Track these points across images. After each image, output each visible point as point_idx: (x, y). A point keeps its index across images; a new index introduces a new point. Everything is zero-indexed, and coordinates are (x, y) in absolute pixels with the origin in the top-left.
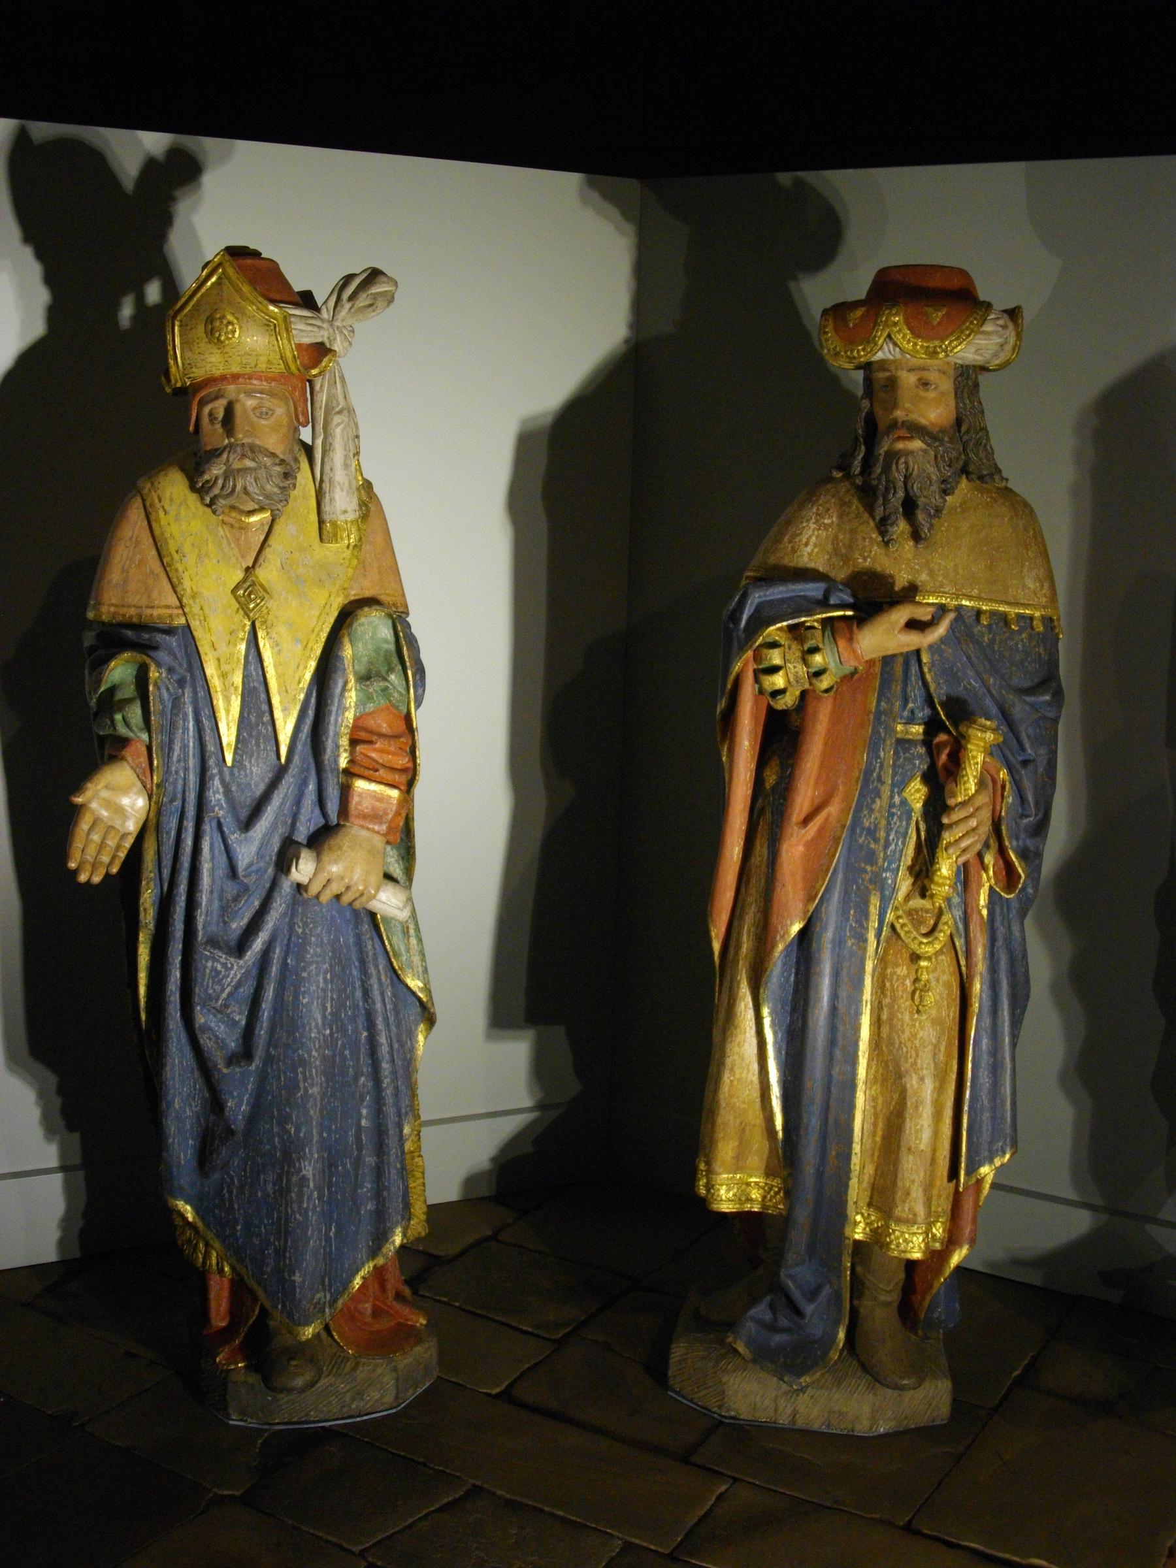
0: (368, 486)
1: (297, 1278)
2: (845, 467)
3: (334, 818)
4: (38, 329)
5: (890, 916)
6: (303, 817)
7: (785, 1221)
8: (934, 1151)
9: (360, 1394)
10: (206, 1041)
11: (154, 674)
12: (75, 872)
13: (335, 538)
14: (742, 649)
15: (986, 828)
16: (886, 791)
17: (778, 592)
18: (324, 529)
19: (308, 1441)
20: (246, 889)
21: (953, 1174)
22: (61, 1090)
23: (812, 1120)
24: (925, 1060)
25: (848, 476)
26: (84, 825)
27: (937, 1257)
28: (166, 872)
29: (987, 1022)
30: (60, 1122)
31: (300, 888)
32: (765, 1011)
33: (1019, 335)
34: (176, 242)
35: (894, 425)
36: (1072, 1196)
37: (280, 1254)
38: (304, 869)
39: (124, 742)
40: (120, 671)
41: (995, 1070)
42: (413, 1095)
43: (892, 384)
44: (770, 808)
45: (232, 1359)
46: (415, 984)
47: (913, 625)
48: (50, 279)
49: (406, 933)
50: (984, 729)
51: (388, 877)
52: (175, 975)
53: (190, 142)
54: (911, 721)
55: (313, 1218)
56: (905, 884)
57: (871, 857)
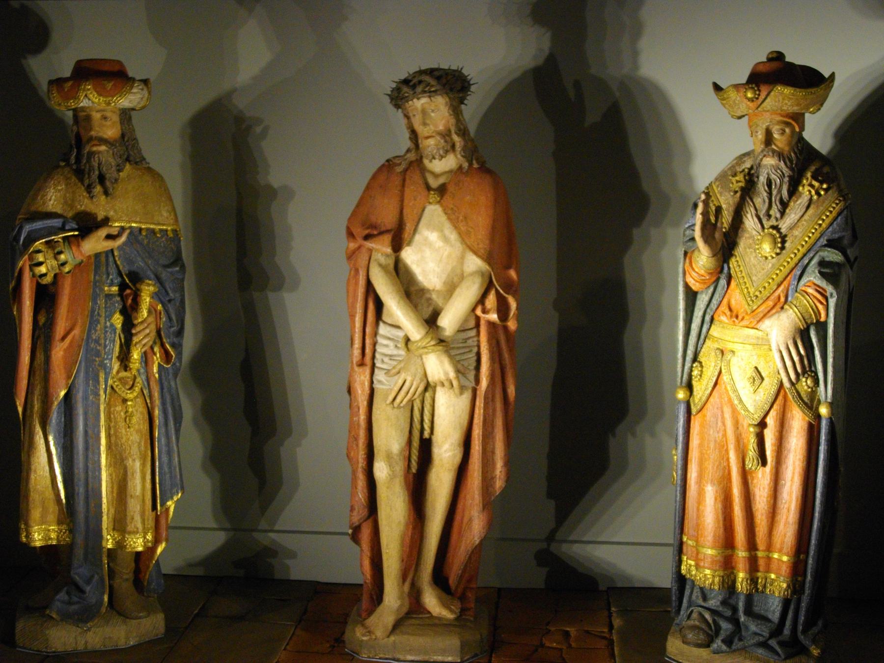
2: (67, 160)
5: (110, 382)
7: (71, 547)
8: (143, 496)
14: (22, 254)
15: (154, 334)
16: (102, 320)
17: (38, 225)
21: (154, 507)
23: (81, 490)
24: (135, 450)
25: (68, 164)
27: (151, 550)
29: (163, 430)
33: (150, 93)
35: (91, 139)
36: (215, 526)
41: (169, 453)
43: (88, 118)
44: (43, 335)
47: (109, 237)
50: (149, 285)
54: (111, 285)
56: (116, 366)
57: (98, 354)
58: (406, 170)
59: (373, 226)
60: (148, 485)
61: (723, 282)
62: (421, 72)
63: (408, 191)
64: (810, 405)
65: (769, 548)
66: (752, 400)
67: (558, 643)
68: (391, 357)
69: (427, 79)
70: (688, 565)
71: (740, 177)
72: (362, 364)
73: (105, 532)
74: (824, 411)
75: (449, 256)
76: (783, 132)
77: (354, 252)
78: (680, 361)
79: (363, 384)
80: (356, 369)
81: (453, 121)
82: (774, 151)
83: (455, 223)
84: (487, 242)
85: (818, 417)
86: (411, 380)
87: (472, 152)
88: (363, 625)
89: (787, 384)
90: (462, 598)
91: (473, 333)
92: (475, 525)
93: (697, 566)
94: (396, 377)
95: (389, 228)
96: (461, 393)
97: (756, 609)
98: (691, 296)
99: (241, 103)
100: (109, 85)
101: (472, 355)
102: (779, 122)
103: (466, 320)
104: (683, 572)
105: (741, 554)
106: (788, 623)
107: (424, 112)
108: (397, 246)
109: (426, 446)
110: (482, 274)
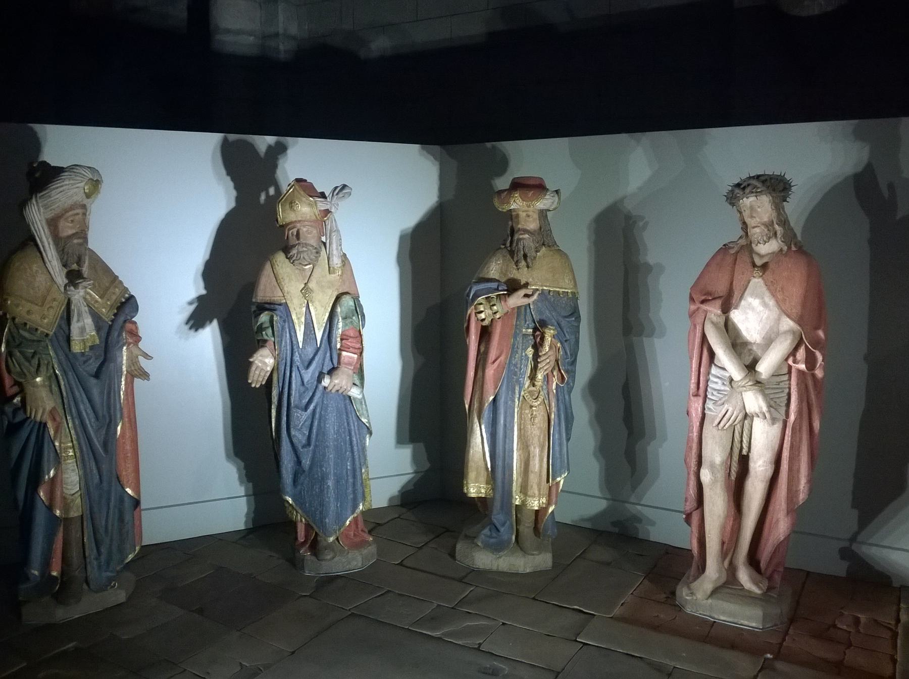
0: (345, 255)
1: (327, 520)
2: (504, 244)
3: (336, 365)
4: (233, 204)
5: (522, 393)
6: (326, 364)
7: (493, 499)
8: (540, 472)
9: (349, 563)
10: (294, 440)
11: (275, 318)
12: (251, 384)
13: (334, 273)
14: (471, 305)
15: (553, 363)
16: (520, 351)
17: (482, 286)
18: (331, 270)
19: (331, 579)
20: (307, 389)
21: (548, 481)
22: (246, 468)
23: (499, 463)
24: (536, 440)
25: (506, 247)
26: (253, 368)
28: (281, 385)
29: (557, 428)
30: (245, 479)
31: (325, 388)
32: (483, 427)
33: (559, 199)
34: (279, 174)
35: (519, 230)
36: (599, 495)
37: (321, 513)
38: (326, 382)
39: (265, 341)
40: (264, 318)
41: (561, 445)
42: (365, 459)
43: (517, 216)
45: (305, 552)
46: (365, 421)
47: (526, 296)
48: (236, 188)
49: (361, 403)
50: (550, 329)
51: (354, 384)
52: (284, 419)
53: (282, 139)
54: (528, 328)
55: (332, 500)
58: (737, 252)
59: (709, 293)
60: (545, 466)
67: (847, 626)
68: (718, 391)
69: (754, 182)
72: (697, 395)
73: (514, 494)
75: (768, 318)
77: (694, 312)
79: (697, 409)
80: (692, 398)
81: (774, 214)
83: (773, 295)
84: (799, 308)
86: (732, 410)
90: (770, 578)
91: (786, 378)
92: (781, 526)
96: (773, 424)
99: (629, 206)
100: (530, 194)
101: (785, 394)
103: (779, 367)
107: (752, 208)
108: (726, 309)
109: (744, 461)
110: (794, 333)
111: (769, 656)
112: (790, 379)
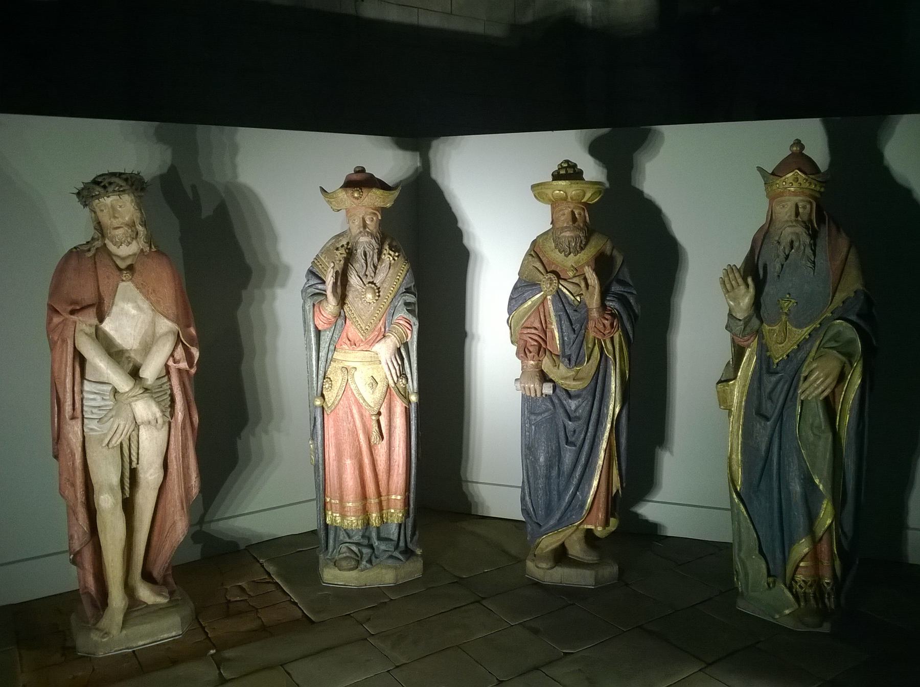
58: (95, 255)
59: (76, 303)
61: (340, 322)
62: (114, 174)
63: (100, 272)
64: (405, 397)
65: (388, 493)
66: (372, 398)
69: (117, 180)
70: (333, 517)
71: (342, 251)
72: (73, 418)
74: (414, 398)
76: (372, 221)
78: (315, 379)
79: (75, 433)
82: (368, 233)
84: (174, 308)
85: (410, 402)
86: (122, 425)
87: (150, 241)
88: (97, 629)
89: (392, 384)
91: (165, 379)
93: (343, 516)
94: (109, 424)
95: (90, 302)
97: (382, 535)
98: (318, 333)
102: (803, 201)
104: (328, 521)
105: (373, 501)
106: (402, 538)
109: (134, 473)
111: (212, 652)
112: (169, 380)
